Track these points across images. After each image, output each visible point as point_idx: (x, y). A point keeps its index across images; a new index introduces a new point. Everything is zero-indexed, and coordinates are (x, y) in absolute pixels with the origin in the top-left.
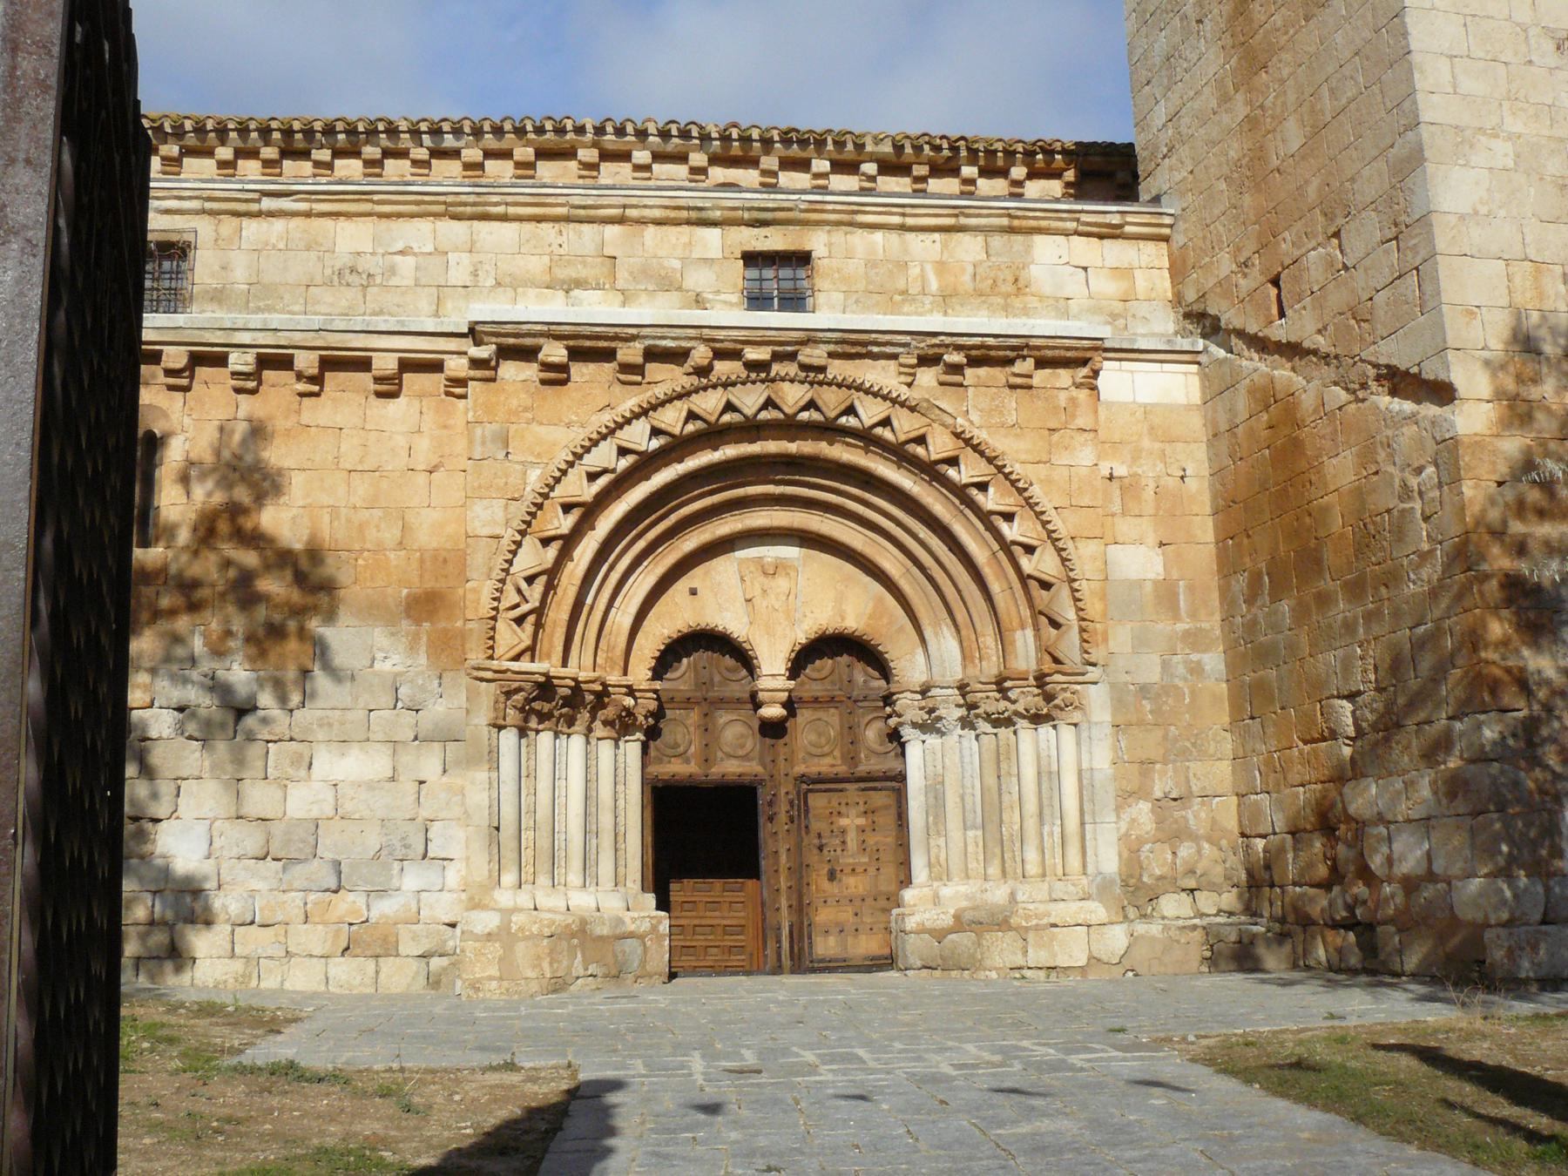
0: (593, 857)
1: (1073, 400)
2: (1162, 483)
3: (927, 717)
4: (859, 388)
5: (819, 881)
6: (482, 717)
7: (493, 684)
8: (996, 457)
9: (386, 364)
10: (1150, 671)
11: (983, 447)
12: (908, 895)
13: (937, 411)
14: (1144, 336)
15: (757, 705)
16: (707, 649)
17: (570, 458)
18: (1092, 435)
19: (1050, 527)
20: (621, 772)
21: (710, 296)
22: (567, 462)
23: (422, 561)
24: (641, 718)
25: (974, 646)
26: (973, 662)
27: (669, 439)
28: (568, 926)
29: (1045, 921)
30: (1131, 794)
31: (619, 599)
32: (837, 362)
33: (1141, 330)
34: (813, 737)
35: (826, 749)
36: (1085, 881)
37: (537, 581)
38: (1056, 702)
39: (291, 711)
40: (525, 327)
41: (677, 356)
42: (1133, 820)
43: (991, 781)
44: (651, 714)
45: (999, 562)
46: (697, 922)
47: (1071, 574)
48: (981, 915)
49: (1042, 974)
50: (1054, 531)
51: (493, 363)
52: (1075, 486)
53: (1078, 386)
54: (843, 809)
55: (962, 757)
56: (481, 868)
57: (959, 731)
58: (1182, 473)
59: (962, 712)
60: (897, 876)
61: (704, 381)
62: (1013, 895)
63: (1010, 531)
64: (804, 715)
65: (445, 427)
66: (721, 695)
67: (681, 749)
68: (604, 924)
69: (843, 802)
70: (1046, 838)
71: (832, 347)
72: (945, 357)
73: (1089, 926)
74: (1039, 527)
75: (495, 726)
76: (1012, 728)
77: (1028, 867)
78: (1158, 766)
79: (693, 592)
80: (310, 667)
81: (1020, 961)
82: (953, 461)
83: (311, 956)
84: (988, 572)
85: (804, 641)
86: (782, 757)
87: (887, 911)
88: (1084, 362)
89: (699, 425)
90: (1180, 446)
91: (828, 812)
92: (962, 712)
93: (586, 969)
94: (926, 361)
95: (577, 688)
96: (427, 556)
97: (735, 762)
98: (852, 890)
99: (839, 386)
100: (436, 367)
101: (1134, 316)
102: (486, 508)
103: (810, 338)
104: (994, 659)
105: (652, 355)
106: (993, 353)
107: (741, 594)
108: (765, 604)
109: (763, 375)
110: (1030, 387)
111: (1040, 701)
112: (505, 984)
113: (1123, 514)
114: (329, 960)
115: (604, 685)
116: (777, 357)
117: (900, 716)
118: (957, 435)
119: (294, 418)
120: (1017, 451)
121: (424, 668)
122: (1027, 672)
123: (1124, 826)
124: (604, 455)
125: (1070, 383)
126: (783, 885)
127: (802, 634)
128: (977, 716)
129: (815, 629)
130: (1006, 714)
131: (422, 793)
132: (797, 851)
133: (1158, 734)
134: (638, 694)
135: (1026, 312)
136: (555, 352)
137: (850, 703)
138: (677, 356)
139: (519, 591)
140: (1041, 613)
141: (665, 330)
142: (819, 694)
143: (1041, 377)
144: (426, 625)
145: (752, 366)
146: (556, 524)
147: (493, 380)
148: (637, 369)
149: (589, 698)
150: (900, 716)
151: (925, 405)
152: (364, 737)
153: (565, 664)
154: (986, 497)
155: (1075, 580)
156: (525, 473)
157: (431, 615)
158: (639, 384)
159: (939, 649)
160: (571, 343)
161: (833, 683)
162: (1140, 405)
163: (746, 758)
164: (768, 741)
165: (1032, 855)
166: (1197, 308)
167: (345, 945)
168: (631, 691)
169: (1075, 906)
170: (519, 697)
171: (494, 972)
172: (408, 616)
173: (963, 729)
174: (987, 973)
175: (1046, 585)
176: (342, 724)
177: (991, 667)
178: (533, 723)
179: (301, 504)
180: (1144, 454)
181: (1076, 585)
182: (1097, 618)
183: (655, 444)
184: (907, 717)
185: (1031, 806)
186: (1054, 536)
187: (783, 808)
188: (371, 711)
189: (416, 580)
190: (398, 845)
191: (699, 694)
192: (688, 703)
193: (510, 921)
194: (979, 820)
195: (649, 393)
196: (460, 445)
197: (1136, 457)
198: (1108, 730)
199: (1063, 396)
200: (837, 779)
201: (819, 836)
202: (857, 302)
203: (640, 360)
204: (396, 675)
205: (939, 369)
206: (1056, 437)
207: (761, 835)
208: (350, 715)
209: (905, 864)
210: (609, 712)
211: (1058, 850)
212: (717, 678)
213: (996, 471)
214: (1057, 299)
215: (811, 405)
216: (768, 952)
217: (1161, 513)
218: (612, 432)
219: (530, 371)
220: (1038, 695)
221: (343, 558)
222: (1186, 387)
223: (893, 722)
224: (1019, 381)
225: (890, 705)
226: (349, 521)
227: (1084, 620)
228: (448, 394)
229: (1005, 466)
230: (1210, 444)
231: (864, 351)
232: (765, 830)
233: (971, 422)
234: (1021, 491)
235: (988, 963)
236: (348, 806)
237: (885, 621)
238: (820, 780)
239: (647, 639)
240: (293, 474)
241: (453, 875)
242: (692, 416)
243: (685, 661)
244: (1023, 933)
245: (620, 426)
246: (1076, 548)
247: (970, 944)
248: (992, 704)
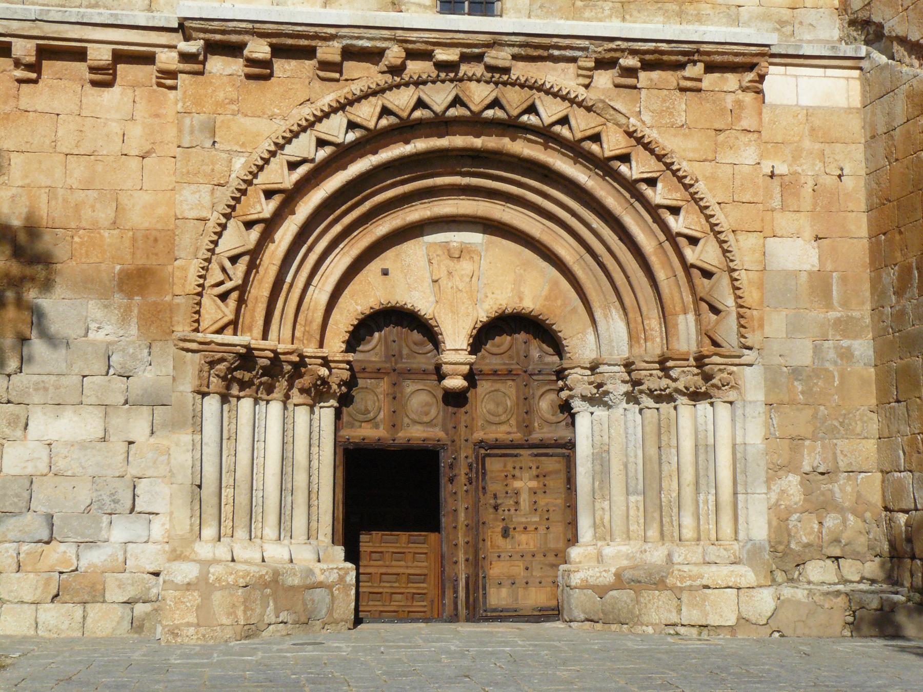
0: (288, 512)
1: (739, 103)
2: (821, 181)
3: (595, 391)
4: (540, 89)
5: (493, 537)
6: (187, 385)
7: (198, 355)
8: (664, 155)
9: (100, 55)
10: (803, 355)
11: (653, 146)
12: (575, 553)
13: (612, 112)
14: (809, 42)
15: (441, 377)
16: (397, 325)
17: (273, 148)
18: (756, 135)
19: (713, 220)
20: (315, 436)
22: (270, 152)
23: (134, 239)
24: (334, 387)
25: (640, 327)
26: (639, 342)
27: (364, 132)
28: (261, 577)
29: (698, 582)
30: (781, 467)
31: (317, 278)
32: (521, 64)
33: (808, 37)
34: (491, 406)
35: (503, 418)
36: (736, 546)
37: (240, 261)
38: (714, 381)
39: (9, 375)
40: (231, 24)
41: (373, 56)
42: (783, 491)
43: (653, 451)
44: (343, 383)
45: (665, 252)
46: (383, 570)
47: (731, 264)
48: (640, 574)
49: (694, 631)
50: (717, 225)
51: (201, 58)
52: (738, 182)
53: (744, 90)
54: (517, 473)
55: (626, 428)
56: (184, 521)
57: (624, 405)
58: (840, 172)
59: (627, 387)
60: (565, 535)
61: (397, 79)
62: (669, 556)
63: (676, 224)
64: (484, 387)
65: (157, 116)
66: (408, 366)
67: (372, 415)
68: (295, 574)
69: (518, 467)
70: (701, 505)
71: (516, 50)
72: (621, 61)
73: (739, 589)
74: (703, 221)
75: (199, 392)
76: (673, 404)
77: (684, 531)
78: (807, 443)
79: (385, 273)
80: (27, 332)
81: (674, 618)
82: (625, 158)
83: (22, 602)
84: (655, 261)
85: (485, 319)
86: (463, 424)
87: (555, 566)
88: (751, 67)
89: (392, 120)
90: (838, 147)
91: (503, 474)
92: (627, 387)
93: (278, 617)
94: (603, 64)
95: (276, 359)
96: (139, 235)
97: (419, 428)
98: (523, 546)
99: (522, 86)
100: (148, 59)
101: (801, 23)
102: (194, 193)
103: (496, 41)
104: (658, 340)
105: (350, 53)
106: (665, 58)
107: (428, 275)
108: (450, 284)
109: (452, 75)
110: (699, 90)
111: (699, 380)
112: (202, 630)
113: (782, 209)
114: (39, 606)
115: (301, 356)
116: (465, 58)
117: (571, 389)
118: (630, 134)
119: (12, 103)
120: (684, 150)
121: (135, 338)
122: (688, 353)
123: (774, 497)
124: (303, 147)
125: (737, 87)
126: (461, 541)
127: (484, 313)
128: (641, 392)
129: (495, 308)
130: (668, 391)
131: (131, 453)
132: (475, 509)
133: (808, 412)
134: (332, 365)
135: (699, 19)
136: (259, 49)
137: (526, 376)
138: (373, 56)
139: (224, 270)
140: (702, 299)
141: (361, 30)
142: (497, 367)
143: (710, 81)
144: (137, 299)
145: (442, 66)
146: (259, 209)
147: (202, 73)
148: (336, 67)
149: (287, 368)
150: (571, 389)
151: (601, 105)
152: (77, 401)
153: (265, 337)
154: (655, 192)
155: (734, 270)
156: (230, 161)
157: (142, 290)
158: (337, 80)
159: (608, 329)
160: (274, 41)
161: (511, 357)
162: (802, 108)
163: (430, 424)
164: (450, 409)
165: (688, 521)
166: (862, 15)
167: (55, 592)
168: (326, 362)
169: (725, 570)
170: (222, 367)
171: (192, 618)
172: (121, 290)
173: (628, 403)
174: (644, 628)
175: (708, 274)
176: (57, 388)
177: (655, 348)
178: (235, 390)
179: (20, 184)
180: (804, 154)
181: (735, 275)
182: (754, 306)
183: (351, 136)
184: (578, 391)
185: (688, 475)
186: (717, 229)
187: (462, 470)
188: (84, 376)
189: (129, 257)
190: (107, 500)
191: (388, 365)
192: (378, 373)
193: (208, 572)
194: (640, 487)
195: (346, 90)
196: (171, 132)
197: (796, 157)
198: (761, 408)
200: (513, 446)
201: (495, 496)
202: (541, 7)
203: (338, 58)
204: (109, 344)
205: (615, 72)
206: (721, 137)
207: (443, 494)
208: (64, 381)
209: (572, 524)
210: (306, 381)
211: (712, 517)
212: (405, 351)
213: (664, 168)
214: (728, 7)
215: (496, 103)
216: (446, 601)
217: (818, 209)
218: (311, 125)
219: (236, 66)
220: (697, 374)
221: (60, 235)
222: (848, 91)
223: (564, 394)
224: (689, 84)
225: (562, 379)
226: (65, 200)
227: (742, 307)
228: (159, 85)
229: (673, 163)
230: (867, 145)
231: (545, 54)
232: (446, 489)
233: (643, 122)
234: (687, 187)
235: (645, 619)
236: (61, 464)
237: (559, 302)
238: (497, 445)
239: (341, 314)
240: (13, 155)
241: (158, 528)
242: (385, 111)
243: (377, 335)
244: (677, 592)
245: (319, 120)
246: (737, 241)
247: (629, 601)
248: (656, 382)
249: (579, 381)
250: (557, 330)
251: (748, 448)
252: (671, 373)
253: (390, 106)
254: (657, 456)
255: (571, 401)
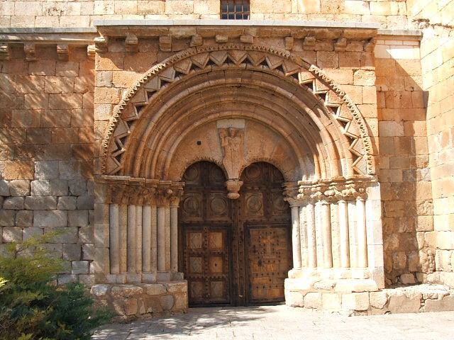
21: (206, 16)
127: (246, 162)
163: (223, 215)
199: (359, 54)
201: (254, 246)
253: (196, 63)
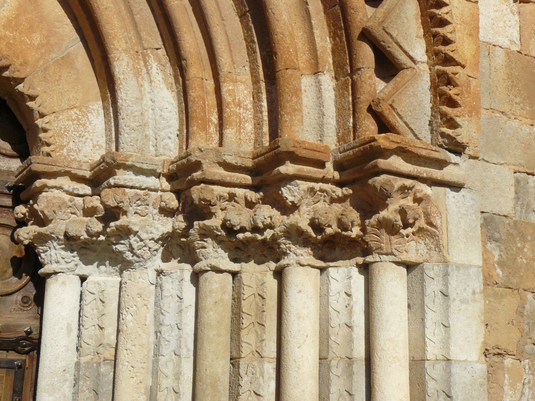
3: (98, 227)
25: (212, 100)
26: (205, 129)
55: (159, 312)
57: (157, 262)
78: (508, 361)
104: (249, 127)
128: (205, 233)
130: (268, 234)
150: (43, 222)
173: (166, 259)
225: (25, 203)
237: (37, 39)
249: (62, 205)
250: (26, 92)
251: (455, 369)
252: (285, 192)
254: (225, 379)
255: (41, 249)
